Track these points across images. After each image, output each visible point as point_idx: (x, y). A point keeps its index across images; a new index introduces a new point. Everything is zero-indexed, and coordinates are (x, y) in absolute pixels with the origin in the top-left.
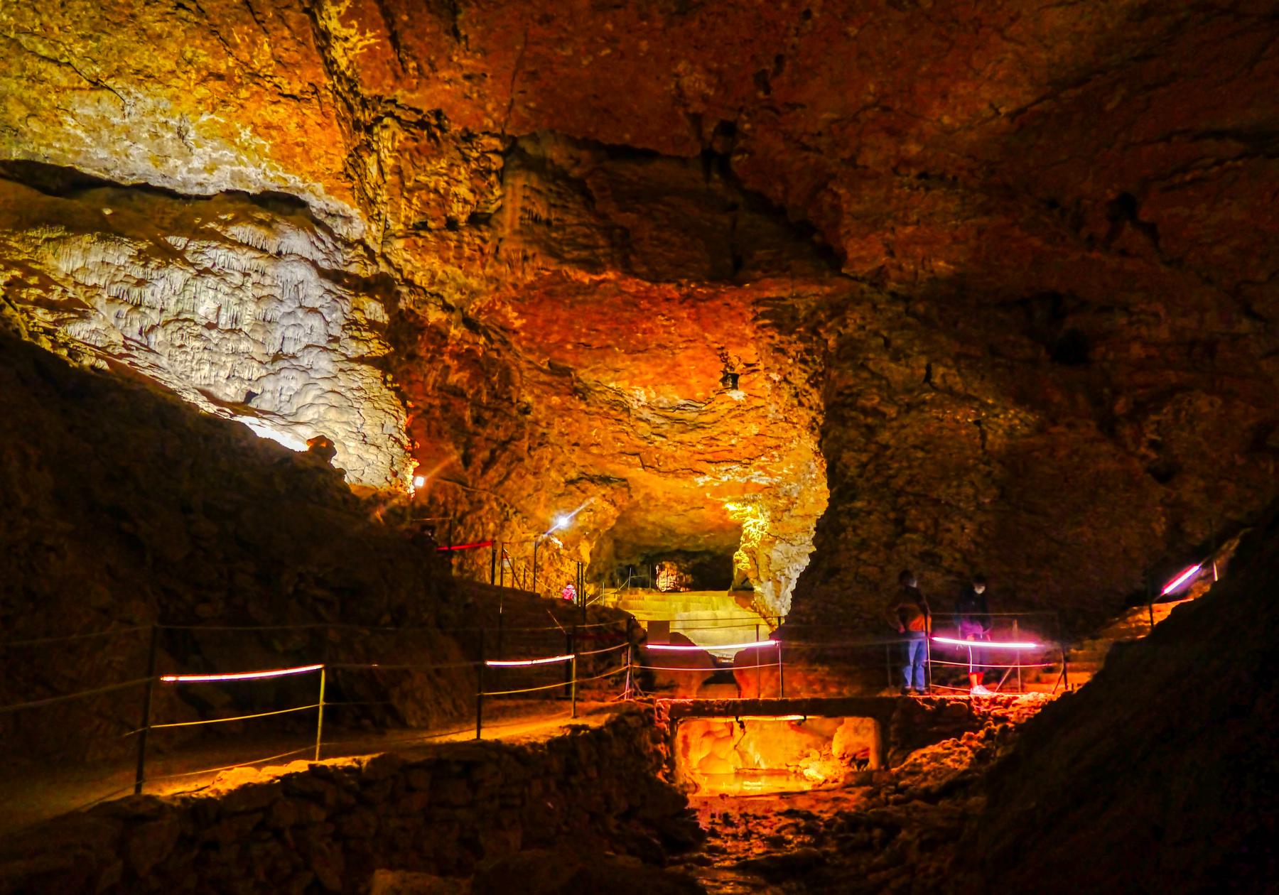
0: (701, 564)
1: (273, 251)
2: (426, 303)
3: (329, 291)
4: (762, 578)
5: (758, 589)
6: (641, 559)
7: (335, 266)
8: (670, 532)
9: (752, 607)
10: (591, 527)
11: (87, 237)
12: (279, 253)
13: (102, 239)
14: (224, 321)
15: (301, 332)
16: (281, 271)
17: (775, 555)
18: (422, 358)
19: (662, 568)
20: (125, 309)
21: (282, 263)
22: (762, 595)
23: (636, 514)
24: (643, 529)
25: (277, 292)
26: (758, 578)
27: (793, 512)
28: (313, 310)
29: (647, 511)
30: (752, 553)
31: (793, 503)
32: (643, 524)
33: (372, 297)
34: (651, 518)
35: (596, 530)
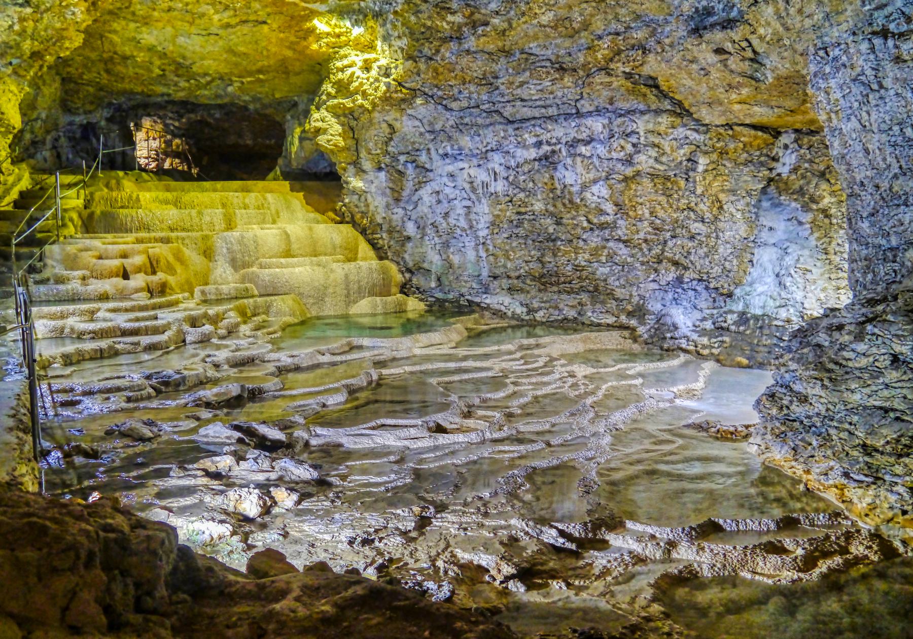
0: (202, 122)
4: (367, 165)
5: (356, 183)
6: (106, 113)
8: (181, 68)
9: (335, 211)
10: (27, 46)
17: (407, 126)
19: (138, 127)
22: (361, 194)
23: (115, 25)
24: (125, 58)
26: (356, 164)
27: (471, 43)
29: (146, 21)
30: (351, 120)
31: (474, 25)
32: (127, 50)
34: (148, 37)
35: (36, 55)
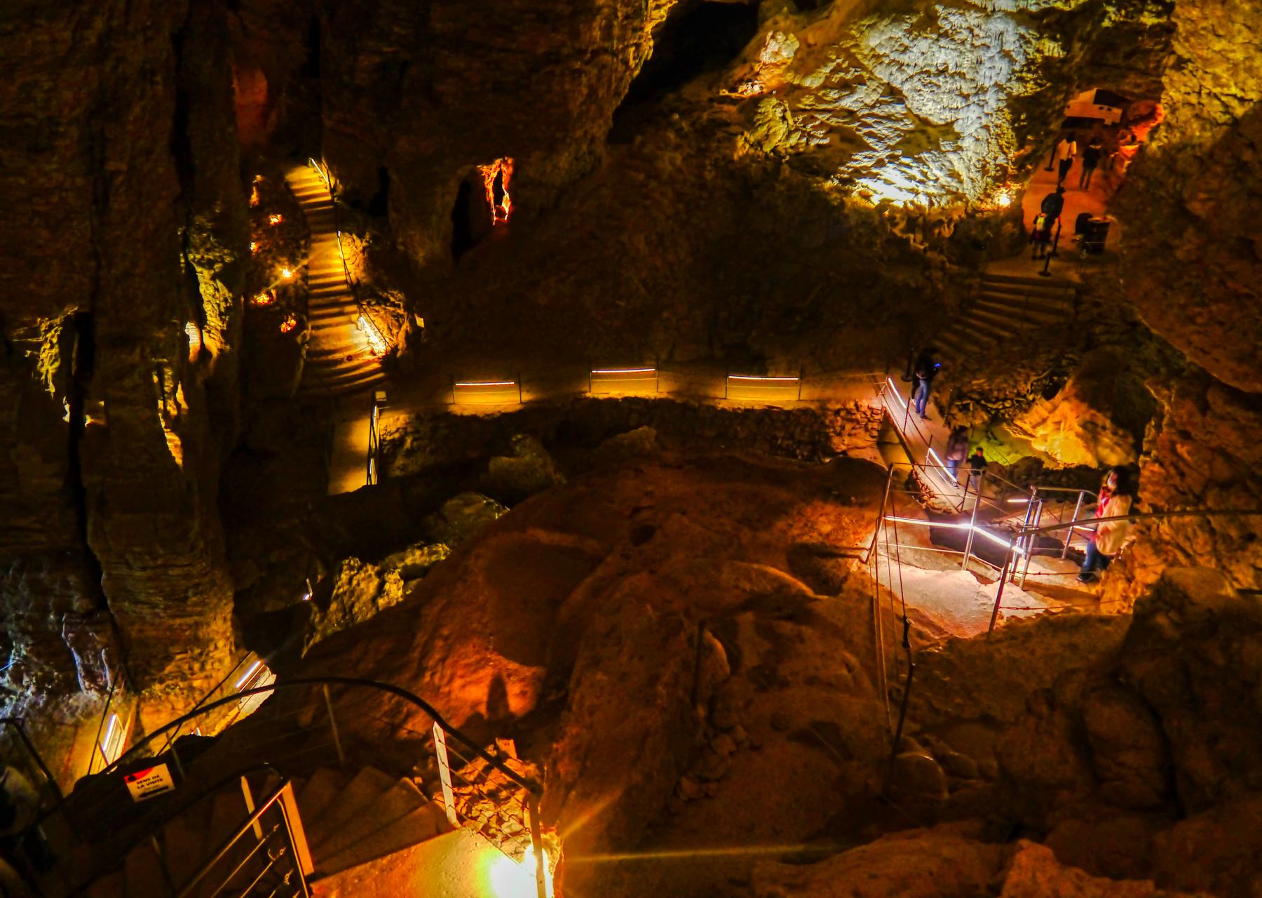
1: (990, 9)
2: (1141, 12)
3: (1022, 37)
7: (1044, 6)
11: (884, 23)
12: (994, 11)
13: (893, 21)
14: (951, 70)
15: (993, 73)
16: (991, 26)
18: (1149, 51)
20: (894, 69)
21: (992, 19)
25: (987, 41)
28: (1006, 55)
33: (1053, 39)
